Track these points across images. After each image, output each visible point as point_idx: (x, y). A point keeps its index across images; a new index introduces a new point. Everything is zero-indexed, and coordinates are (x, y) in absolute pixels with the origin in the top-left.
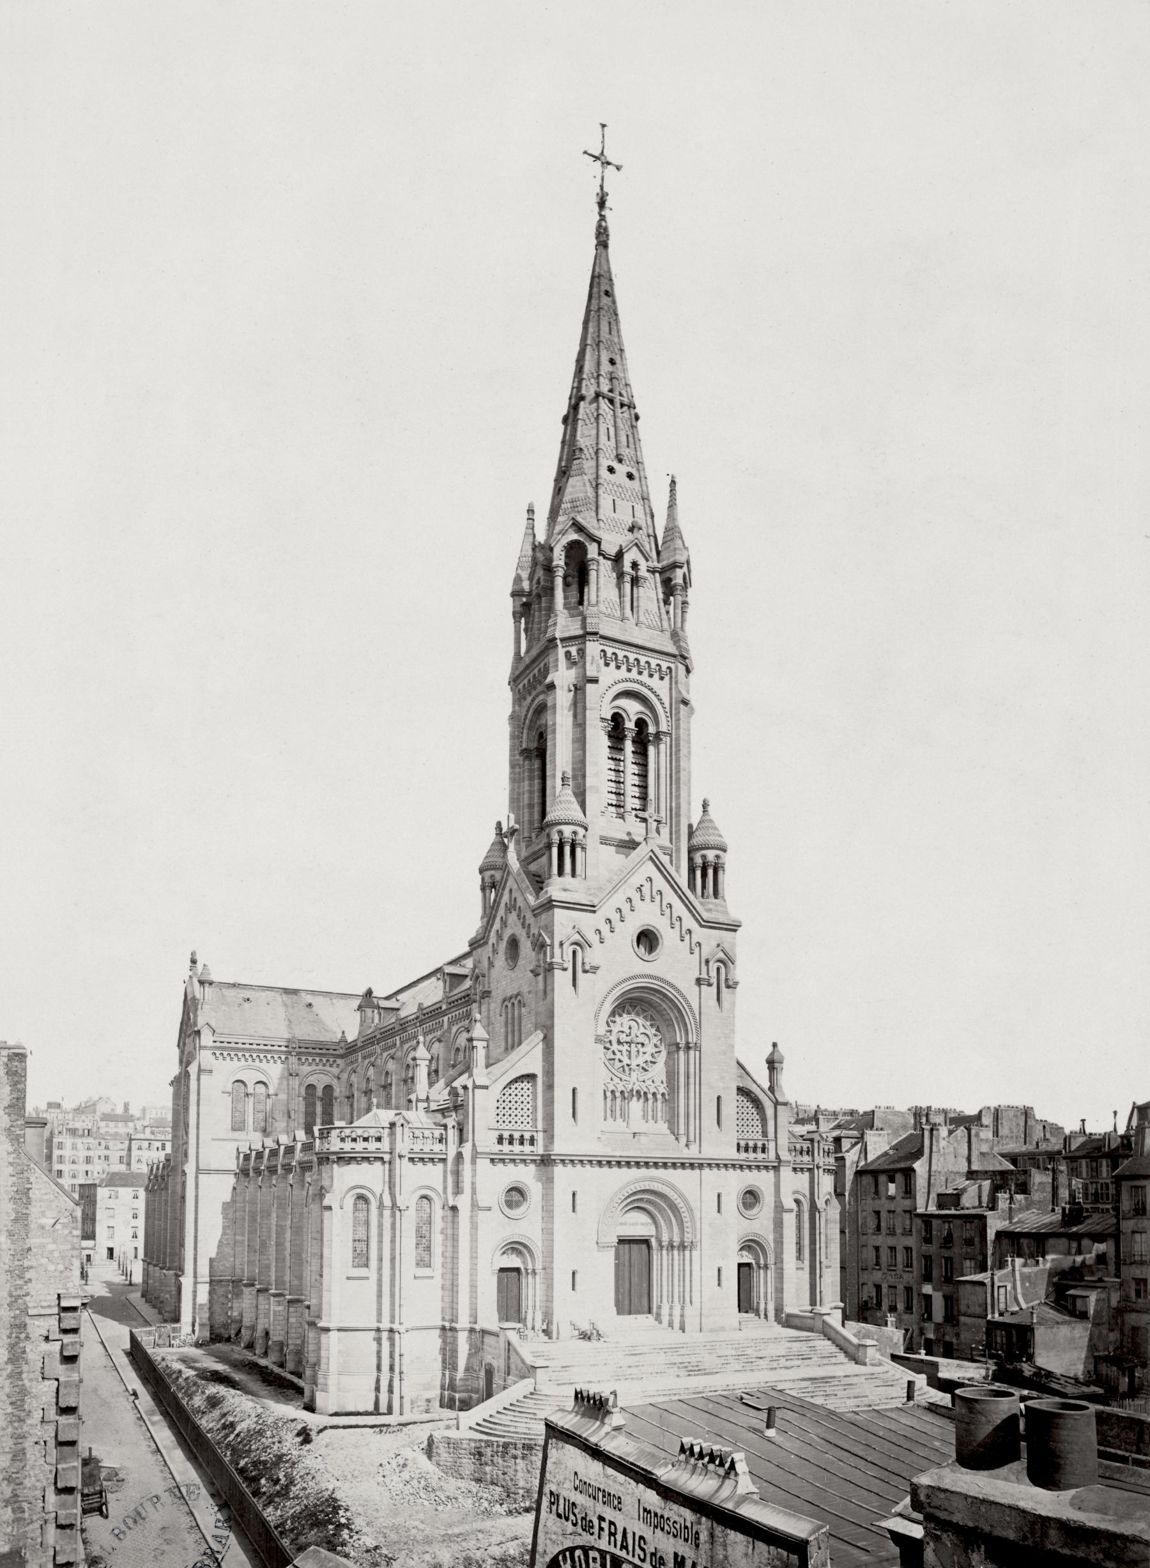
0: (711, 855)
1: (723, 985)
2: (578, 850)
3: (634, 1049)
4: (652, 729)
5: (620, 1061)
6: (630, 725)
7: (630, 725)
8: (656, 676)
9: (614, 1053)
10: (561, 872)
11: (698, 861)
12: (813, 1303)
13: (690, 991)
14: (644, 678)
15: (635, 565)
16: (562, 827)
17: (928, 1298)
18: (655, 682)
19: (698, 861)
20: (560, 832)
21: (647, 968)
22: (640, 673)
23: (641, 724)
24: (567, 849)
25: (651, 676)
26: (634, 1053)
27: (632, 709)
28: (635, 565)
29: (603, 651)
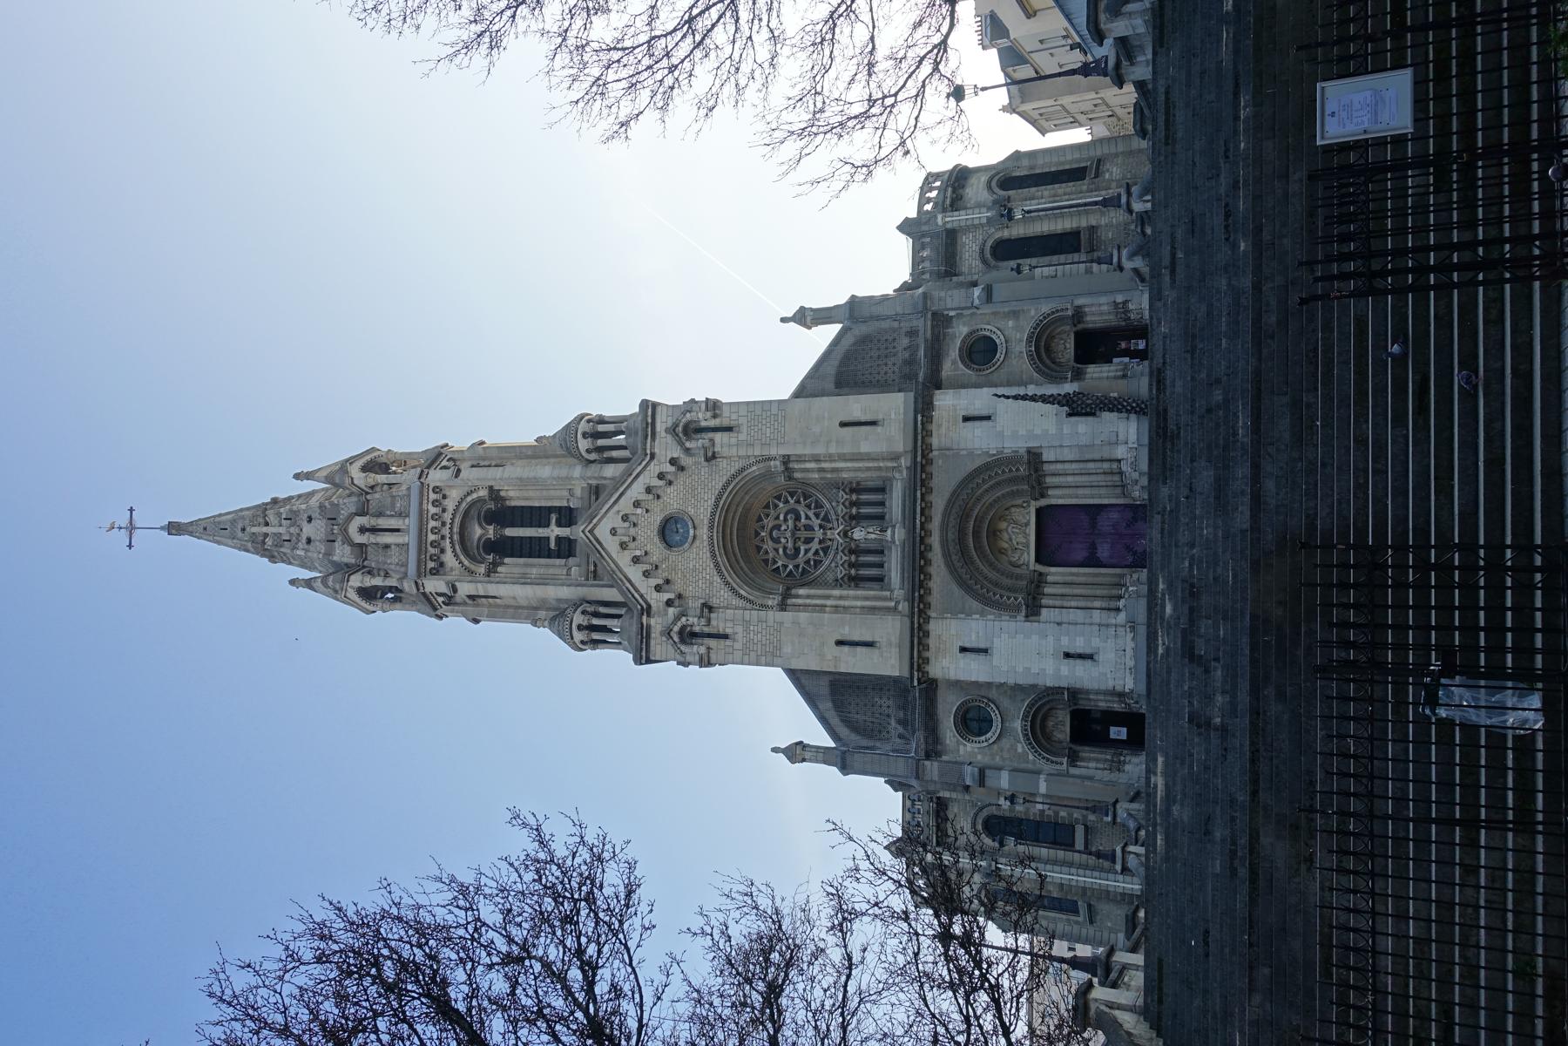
1: (713, 423)
3: (803, 534)
4: (492, 506)
5: (816, 553)
9: (808, 562)
11: (593, 456)
13: (725, 469)
14: (447, 517)
15: (362, 530)
18: (450, 505)
21: (704, 532)
26: (809, 534)
28: (362, 530)
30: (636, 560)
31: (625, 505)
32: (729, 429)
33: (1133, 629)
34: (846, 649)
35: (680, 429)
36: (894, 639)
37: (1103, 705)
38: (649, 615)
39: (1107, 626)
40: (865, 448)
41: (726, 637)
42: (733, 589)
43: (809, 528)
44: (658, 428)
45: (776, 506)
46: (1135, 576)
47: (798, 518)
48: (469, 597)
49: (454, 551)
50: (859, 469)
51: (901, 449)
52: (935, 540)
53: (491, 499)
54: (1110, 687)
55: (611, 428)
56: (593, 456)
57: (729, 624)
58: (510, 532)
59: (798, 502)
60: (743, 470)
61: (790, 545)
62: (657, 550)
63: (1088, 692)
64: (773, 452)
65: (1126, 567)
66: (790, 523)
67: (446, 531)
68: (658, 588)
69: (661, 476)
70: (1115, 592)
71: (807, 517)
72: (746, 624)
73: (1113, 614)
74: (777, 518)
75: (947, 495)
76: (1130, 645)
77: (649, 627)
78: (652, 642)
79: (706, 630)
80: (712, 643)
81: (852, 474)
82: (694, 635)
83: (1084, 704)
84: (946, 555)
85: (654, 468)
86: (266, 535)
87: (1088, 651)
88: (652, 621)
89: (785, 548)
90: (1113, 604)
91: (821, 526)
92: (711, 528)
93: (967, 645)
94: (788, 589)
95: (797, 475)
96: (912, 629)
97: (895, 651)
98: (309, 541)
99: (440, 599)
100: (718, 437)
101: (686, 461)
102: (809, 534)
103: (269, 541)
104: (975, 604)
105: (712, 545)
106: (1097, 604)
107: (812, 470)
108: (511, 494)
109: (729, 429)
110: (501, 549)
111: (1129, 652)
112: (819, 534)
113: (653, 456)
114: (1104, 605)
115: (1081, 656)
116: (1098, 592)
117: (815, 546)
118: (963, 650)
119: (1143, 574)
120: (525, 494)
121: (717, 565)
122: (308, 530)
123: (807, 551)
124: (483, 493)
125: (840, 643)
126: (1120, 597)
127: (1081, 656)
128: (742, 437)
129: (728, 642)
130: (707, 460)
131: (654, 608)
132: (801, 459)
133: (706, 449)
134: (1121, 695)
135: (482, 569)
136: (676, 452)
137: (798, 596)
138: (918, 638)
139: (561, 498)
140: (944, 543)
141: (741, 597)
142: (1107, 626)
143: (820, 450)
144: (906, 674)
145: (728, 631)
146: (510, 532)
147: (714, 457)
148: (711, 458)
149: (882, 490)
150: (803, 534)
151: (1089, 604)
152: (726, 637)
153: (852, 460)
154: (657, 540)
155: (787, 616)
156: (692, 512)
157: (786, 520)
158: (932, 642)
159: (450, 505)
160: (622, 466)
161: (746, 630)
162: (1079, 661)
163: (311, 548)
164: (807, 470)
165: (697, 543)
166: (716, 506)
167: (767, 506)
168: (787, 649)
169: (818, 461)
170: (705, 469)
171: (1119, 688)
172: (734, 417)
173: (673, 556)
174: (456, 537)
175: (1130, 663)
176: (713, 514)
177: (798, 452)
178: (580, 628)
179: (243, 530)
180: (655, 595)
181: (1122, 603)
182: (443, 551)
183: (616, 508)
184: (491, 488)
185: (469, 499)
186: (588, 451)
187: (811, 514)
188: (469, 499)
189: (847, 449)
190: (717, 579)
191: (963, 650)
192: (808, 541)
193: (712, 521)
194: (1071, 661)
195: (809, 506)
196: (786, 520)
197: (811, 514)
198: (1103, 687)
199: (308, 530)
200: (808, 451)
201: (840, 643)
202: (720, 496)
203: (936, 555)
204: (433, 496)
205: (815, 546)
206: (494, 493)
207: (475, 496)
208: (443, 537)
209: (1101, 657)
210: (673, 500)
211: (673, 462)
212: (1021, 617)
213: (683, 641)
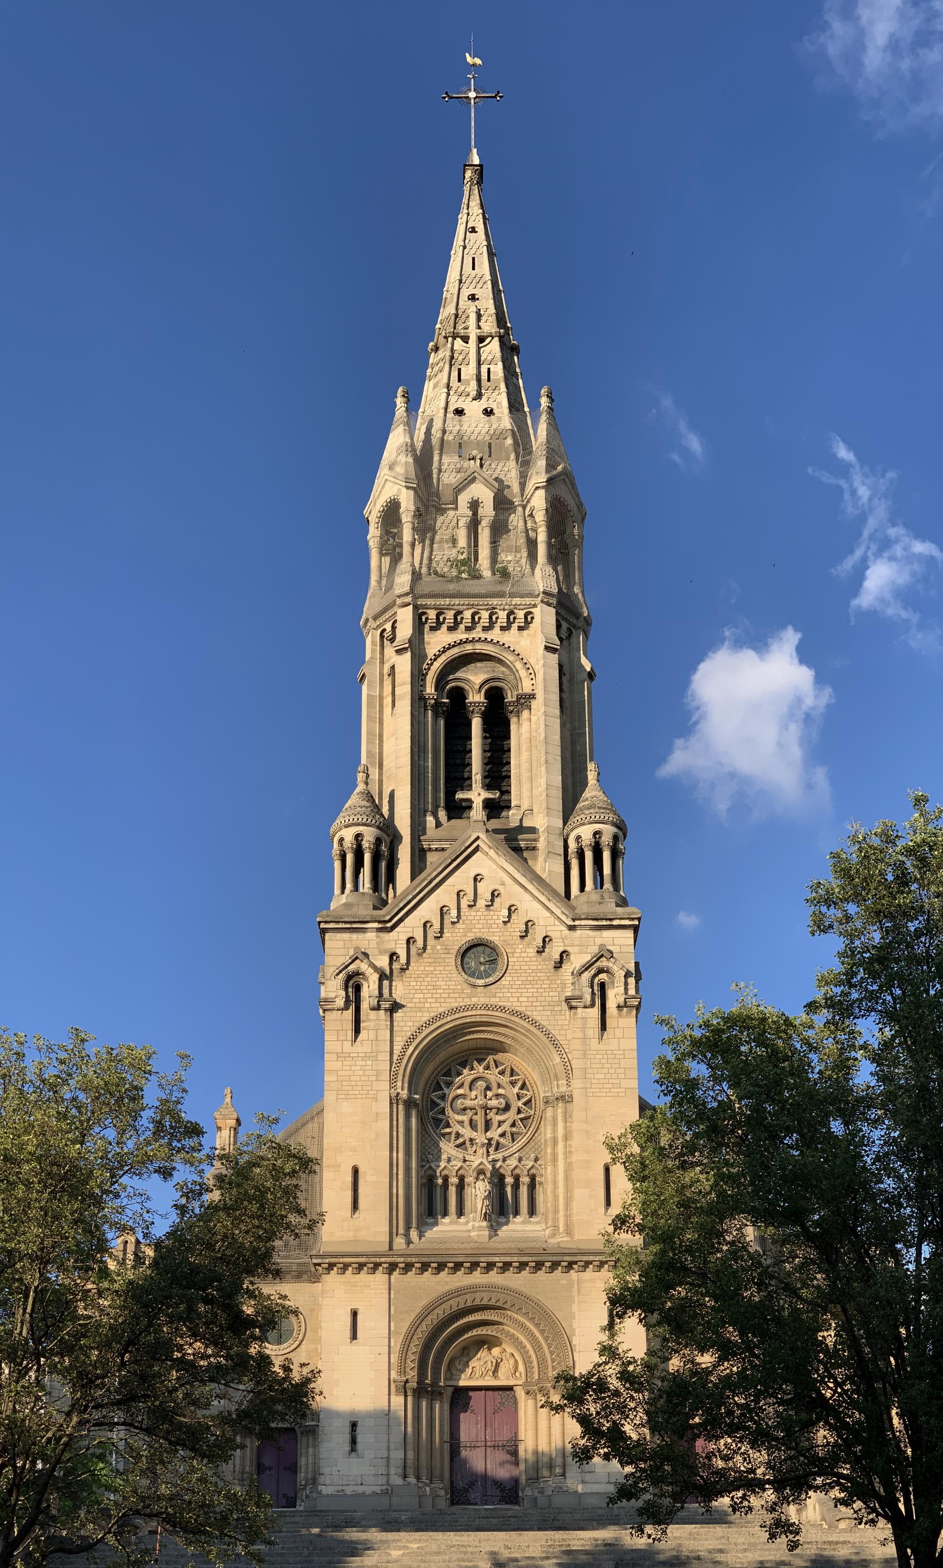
1: (611, 1004)
4: (510, 697)
5: (458, 1135)
21: (481, 998)
23: (495, 695)
30: (443, 912)
31: (513, 893)
32: (603, 1027)
33: (385, 1493)
34: (349, 1178)
35: (603, 963)
36: (363, 1235)
37: (302, 1461)
38: (379, 930)
39: (388, 1466)
40: (579, 1193)
41: (357, 1031)
42: (413, 1037)
43: (488, 1126)
44: (606, 933)
45: (513, 1083)
46: (442, 1493)
47: (499, 1111)
48: (393, 667)
49: (450, 647)
50: (555, 1183)
51: (577, 1237)
52: (478, 1277)
53: (519, 697)
54: (323, 1470)
55: (607, 870)
56: (572, 845)
57: (372, 1035)
59: (519, 1112)
60: (555, 1044)
61: (468, 1103)
62: (457, 938)
63: (315, 1446)
64: (576, 1083)
65: (452, 1482)
66: (494, 1103)
67: (477, 633)
68: (410, 941)
69: (546, 940)
70: (424, 1472)
71: (500, 1123)
72: (372, 1056)
73: (400, 1471)
74: (499, 1086)
75: (526, 1291)
76: (368, 1490)
77: (364, 930)
78: (346, 936)
79: (364, 1006)
80: (349, 1014)
81: (550, 1178)
82: (358, 988)
83: (302, 1441)
84: (459, 1292)
85: (558, 931)
87: (360, 1446)
88: (371, 935)
89: (463, 1096)
90: (410, 1471)
91: (490, 1140)
92: (487, 1007)
93: (360, 1318)
94: (416, 1105)
95: (549, 1112)
96: (375, 1256)
97: (350, 1235)
98: (459, 412)
99: (388, 627)
100: (595, 1012)
101: (568, 968)
102: (481, 1125)
103: (459, 343)
104: (405, 1326)
105: (467, 1008)
106: (411, 1455)
107: (555, 1130)
108: (525, 726)
109: (603, 1027)
111: (360, 1489)
112: (481, 1138)
113: (572, 928)
114: (409, 1463)
115: (353, 1441)
116: (423, 1456)
117: (467, 1132)
118: (355, 1314)
119: (443, 1503)
120: (524, 747)
121: (441, 1016)
122: (474, 409)
123: (461, 1123)
124: (526, 687)
125: (356, 1171)
126: (418, 1478)
127: (353, 1441)
128: (594, 1043)
129: (350, 1034)
130: (567, 1000)
131: (386, 936)
132: (567, 1116)
133: (579, 998)
134: (314, 1481)
135: (430, 689)
136: (577, 960)
137: (408, 1117)
138: (364, 1263)
139: (520, 798)
140: (473, 1289)
141: (405, 1047)
142: (388, 1466)
143: (575, 1142)
144: (323, 1249)
145: (363, 1035)
147: (571, 1008)
148: (570, 1003)
149: (532, 1212)
150: (479, 1119)
151: (410, 1446)
152: (357, 1031)
153: (567, 1178)
154: (471, 936)
155: (384, 1106)
156: (503, 981)
157: (497, 1096)
158: (364, 1276)
159: (511, 638)
160: (561, 889)
161: (366, 1057)
162: (348, 1437)
163: (450, 415)
164: (555, 1124)
165: (469, 990)
166: (514, 1013)
167: (512, 1073)
168: (346, 1107)
169: (566, 1138)
170: (556, 996)
171: (321, 1479)
172: (618, 1033)
173: (452, 960)
174: (469, 648)
175: (349, 1491)
176: (503, 1009)
177: (576, 1115)
178: (358, 837)
179: (473, 298)
180: (404, 938)
181: (412, 1480)
182: (450, 629)
183: (509, 881)
184: (532, 696)
185: (519, 665)
186: (578, 838)
187: (505, 1127)
188: (519, 665)
189: (576, 1174)
190: (426, 1017)
191: (355, 1314)
192: (473, 1125)
193: (495, 1008)
194: (348, 1430)
195: (513, 1125)
196: (497, 1096)
197: (505, 1127)
198: (322, 1463)
199: (474, 409)
200: (575, 1126)
201: (356, 1171)
202: (524, 1017)
203: (461, 1279)
205: (467, 1132)
206: (526, 700)
207: (523, 673)
209: (354, 1460)
210: (520, 956)
211: (564, 954)
212: (394, 1375)
213: (349, 977)
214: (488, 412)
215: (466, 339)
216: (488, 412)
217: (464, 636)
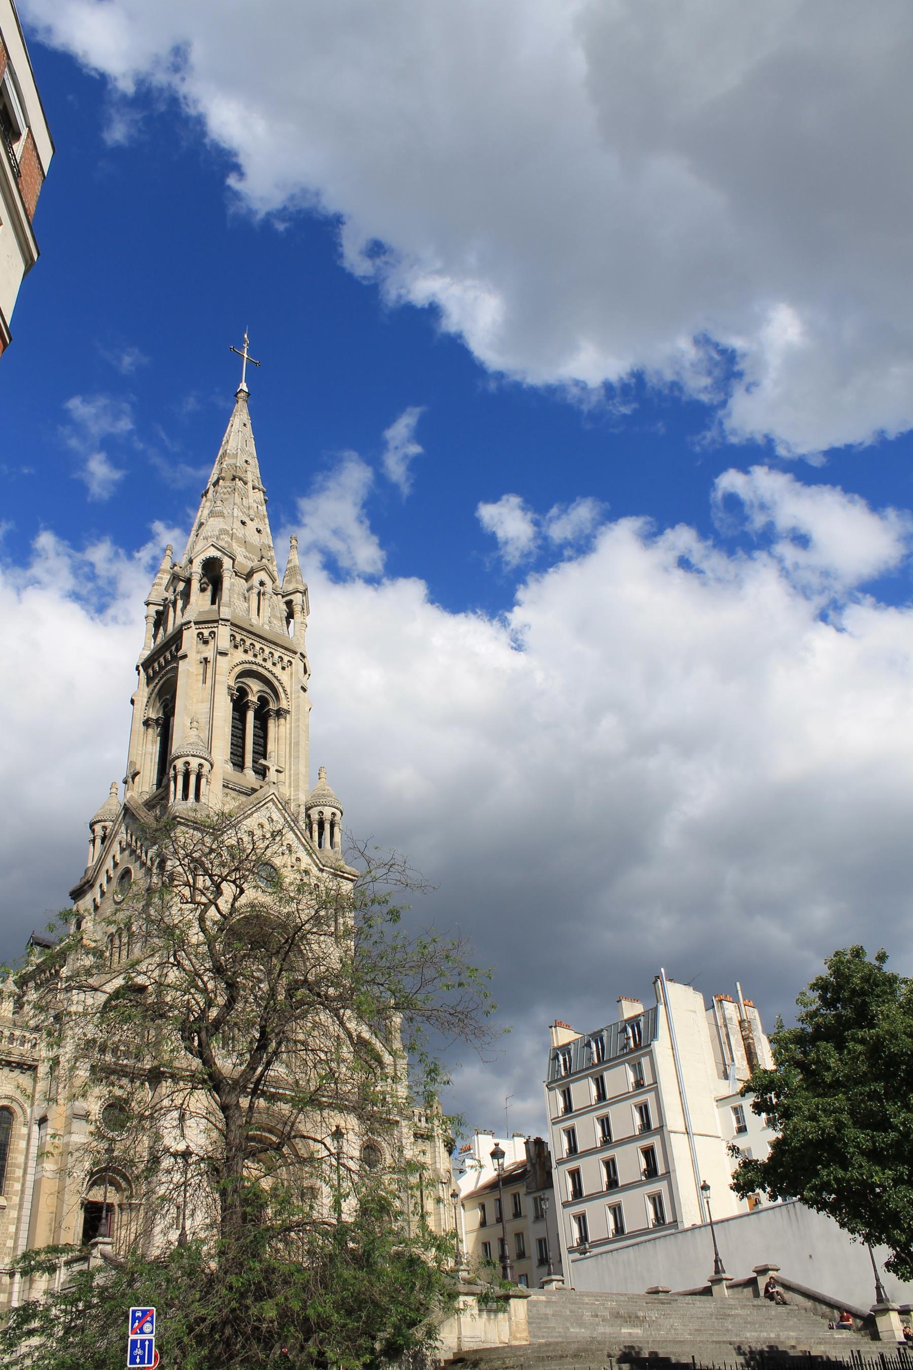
0: (328, 812)
2: (203, 781)
4: (272, 706)
6: (253, 698)
7: (253, 698)
8: (279, 666)
10: (185, 796)
11: (315, 816)
12: (499, 1200)
14: (269, 664)
15: (262, 584)
16: (189, 759)
17: (415, 1284)
18: (277, 670)
19: (315, 816)
20: (187, 763)
22: (265, 660)
23: (263, 701)
24: (193, 779)
25: (274, 664)
27: (255, 687)
29: (232, 635)
58: (250, 715)
67: (259, 660)
86: (246, 483)
108: (282, 729)
110: (240, 704)
124: (284, 704)
146: (250, 715)
178: (201, 765)
184: (288, 712)
185: (280, 690)
204: (286, 659)
207: (282, 695)
208: (255, 656)
214: (259, 531)
215: (246, 483)
216: (259, 531)
217: (253, 659)
